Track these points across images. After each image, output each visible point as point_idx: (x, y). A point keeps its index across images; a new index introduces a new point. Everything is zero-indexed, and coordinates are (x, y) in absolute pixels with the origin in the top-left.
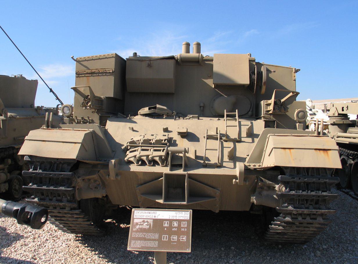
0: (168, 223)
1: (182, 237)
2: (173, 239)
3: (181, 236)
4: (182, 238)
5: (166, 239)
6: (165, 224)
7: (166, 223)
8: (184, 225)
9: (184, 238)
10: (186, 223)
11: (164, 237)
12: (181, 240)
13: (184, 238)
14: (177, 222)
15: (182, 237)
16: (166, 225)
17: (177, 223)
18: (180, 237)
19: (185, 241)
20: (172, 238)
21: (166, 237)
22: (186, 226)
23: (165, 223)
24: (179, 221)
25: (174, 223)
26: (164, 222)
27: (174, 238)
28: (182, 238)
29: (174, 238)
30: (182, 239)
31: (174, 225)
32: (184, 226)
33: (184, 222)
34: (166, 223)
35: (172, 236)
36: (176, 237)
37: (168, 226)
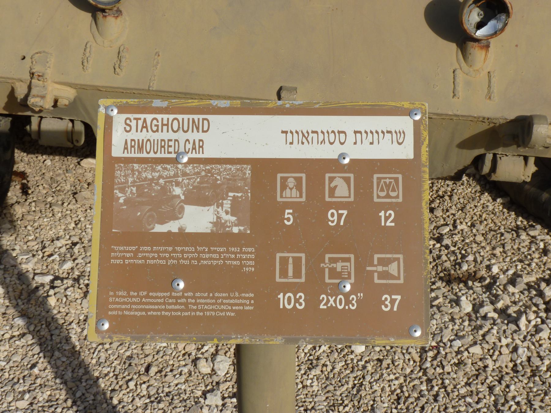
0: (298, 180)
1: (382, 262)
2: (334, 274)
3: (376, 256)
4: (380, 268)
5: (298, 273)
6: (284, 187)
7: (291, 183)
8: (387, 193)
9: (393, 269)
10: (396, 180)
11: (284, 261)
12: (376, 281)
13: (393, 269)
14: (352, 176)
15: (382, 262)
16: (291, 195)
17: (347, 180)
18: (373, 265)
19: (401, 281)
20: (326, 265)
21: (297, 261)
22: (400, 200)
23: (284, 180)
24: (364, 171)
25: (331, 179)
26: (279, 175)
27: (339, 266)
28: (380, 268)
29: (339, 266)
30: (385, 275)
31: (332, 191)
32: (388, 196)
33: (388, 177)
34: (291, 183)
35: (327, 256)
36: (348, 260)
37: (304, 199)
